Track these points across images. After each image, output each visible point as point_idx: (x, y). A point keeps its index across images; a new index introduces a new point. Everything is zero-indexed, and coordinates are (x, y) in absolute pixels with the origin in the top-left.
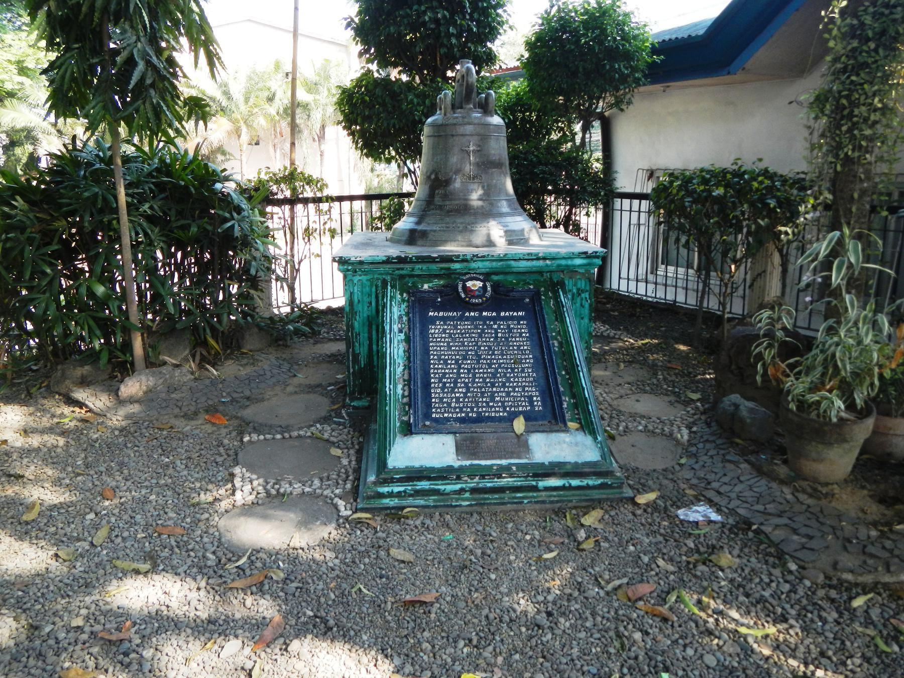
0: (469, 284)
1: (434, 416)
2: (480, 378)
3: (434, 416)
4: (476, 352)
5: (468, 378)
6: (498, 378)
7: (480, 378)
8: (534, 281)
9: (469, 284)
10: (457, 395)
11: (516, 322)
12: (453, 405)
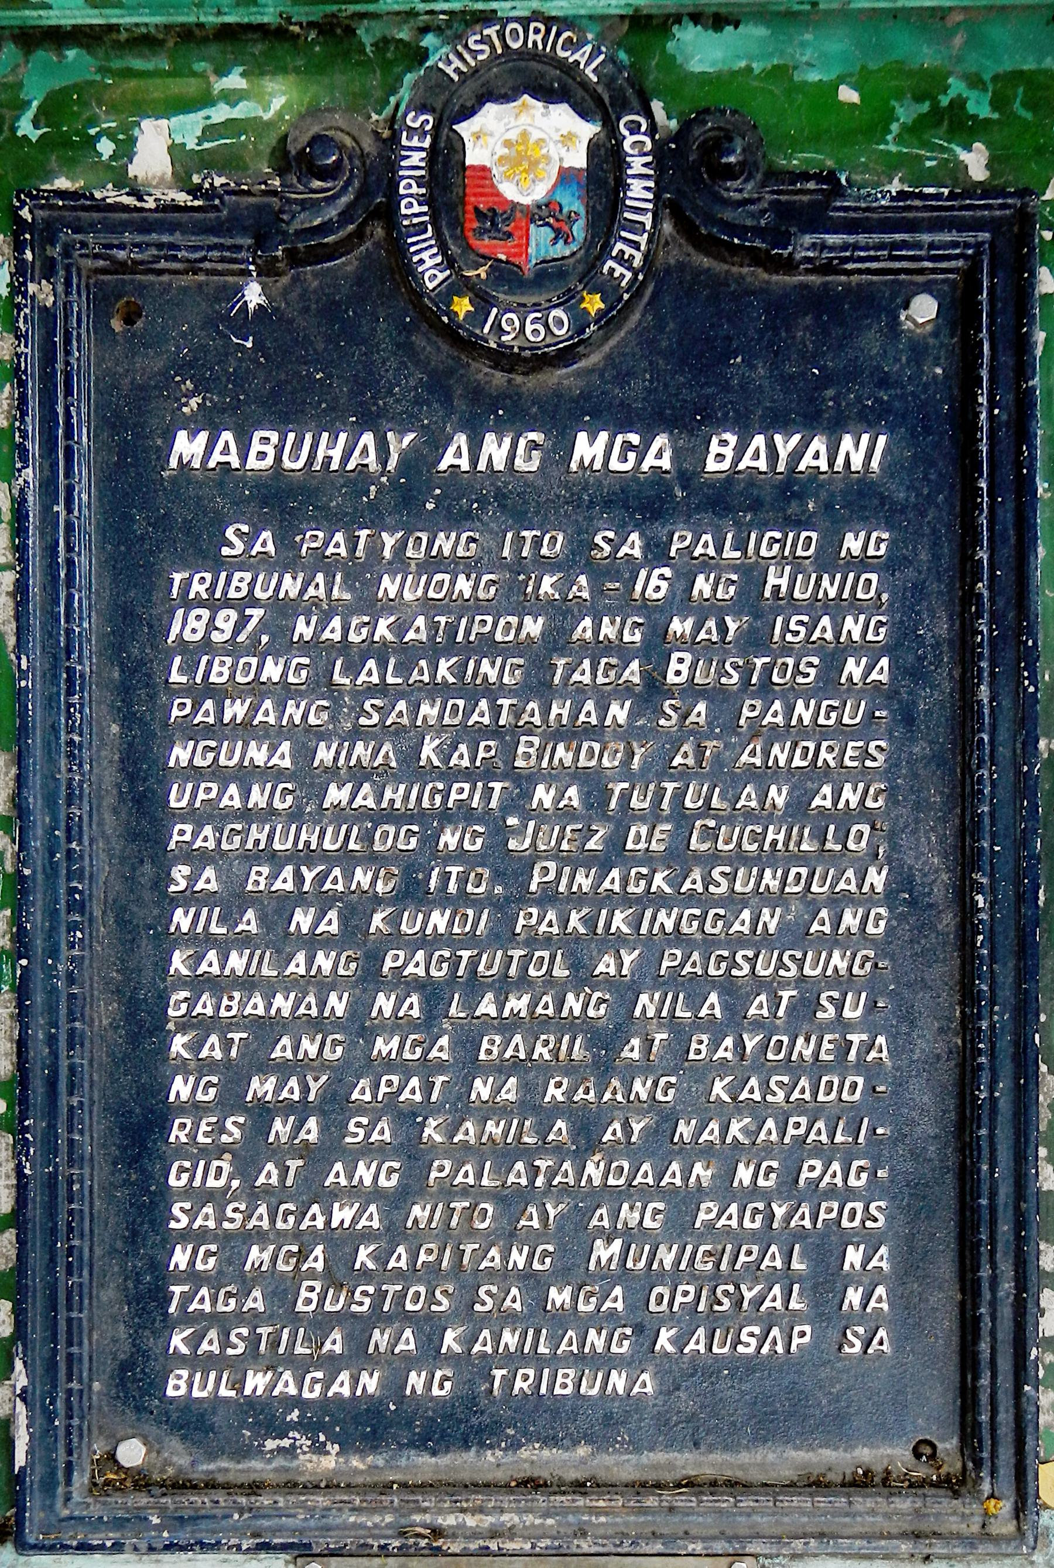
0: (490, 135)
1: (176, 1387)
2: (503, 1069)
3: (176, 1387)
4: (499, 832)
5: (427, 1068)
7: (503, 1069)
8: (1003, 88)
9: (490, 135)
10: (342, 1215)
11: (807, 542)
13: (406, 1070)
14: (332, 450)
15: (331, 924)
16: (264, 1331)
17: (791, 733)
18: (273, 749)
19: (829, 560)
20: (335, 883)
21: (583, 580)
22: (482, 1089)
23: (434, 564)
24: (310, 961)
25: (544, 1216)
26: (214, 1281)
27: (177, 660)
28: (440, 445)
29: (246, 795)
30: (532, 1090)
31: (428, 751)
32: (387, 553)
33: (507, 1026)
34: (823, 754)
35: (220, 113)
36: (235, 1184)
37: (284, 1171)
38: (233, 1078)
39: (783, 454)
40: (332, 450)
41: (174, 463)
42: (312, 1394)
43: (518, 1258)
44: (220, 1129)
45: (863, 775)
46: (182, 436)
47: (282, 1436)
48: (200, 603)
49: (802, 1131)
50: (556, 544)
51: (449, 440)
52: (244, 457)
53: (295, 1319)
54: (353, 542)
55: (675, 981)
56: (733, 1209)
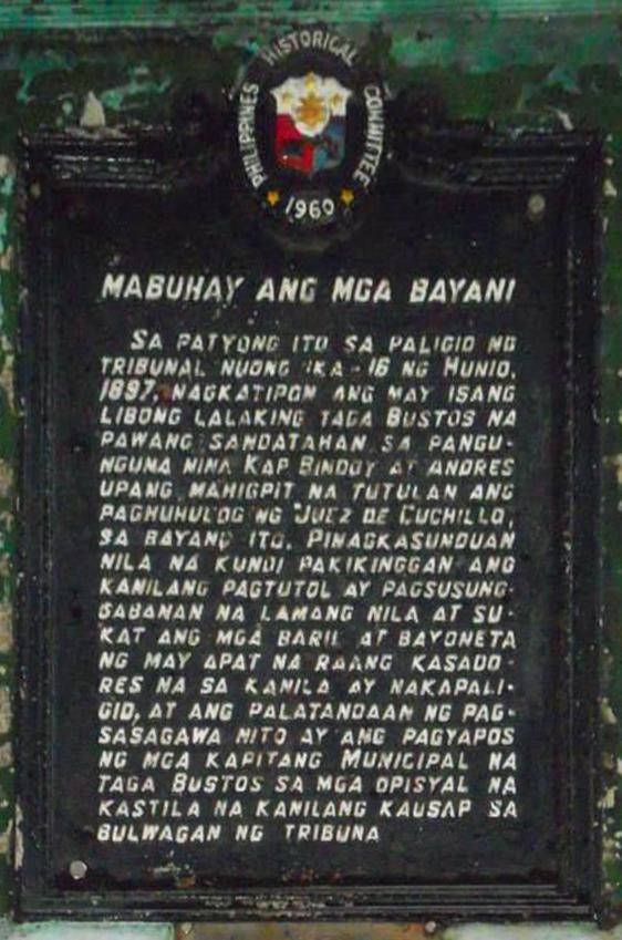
0: (289, 97)
1: (103, 835)
2: (290, 651)
3: (103, 835)
4: (289, 514)
5: (248, 650)
6: (365, 653)
7: (290, 651)
9: (289, 97)
10: (199, 735)
12: (179, 784)
13: (233, 649)
14: (195, 288)
15: (192, 566)
16: (154, 803)
17: (460, 456)
18: (159, 464)
19: (481, 354)
20: (195, 542)
21: (339, 365)
22: (279, 662)
23: (253, 355)
24: (181, 587)
25: (315, 735)
26: (124, 773)
27: (105, 410)
28: (253, 286)
29: (144, 489)
30: (307, 665)
31: (250, 461)
32: (226, 348)
33: (293, 626)
34: (477, 467)
35: (134, 88)
36: (137, 717)
37: (165, 709)
38: (136, 654)
39: (455, 292)
40: (195, 288)
41: (104, 294)
42: (181, 840)
43: (301, 760)
44: (128, 685)
45: (499, 479)
46: (109, 278)
47: (164, 865)
48: (117, 376)
49: (465, 687)
50: (322, 343)
51: (262, 283)
52: (144, 290)
53: (172, 797)
54: (206, 341)
55: (390, 600)
56: (425, 732)
